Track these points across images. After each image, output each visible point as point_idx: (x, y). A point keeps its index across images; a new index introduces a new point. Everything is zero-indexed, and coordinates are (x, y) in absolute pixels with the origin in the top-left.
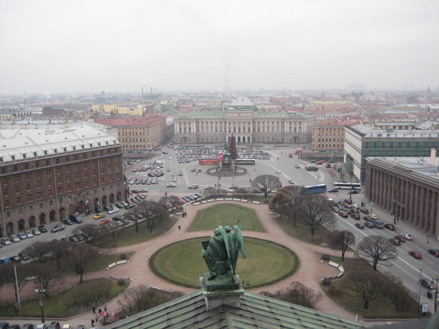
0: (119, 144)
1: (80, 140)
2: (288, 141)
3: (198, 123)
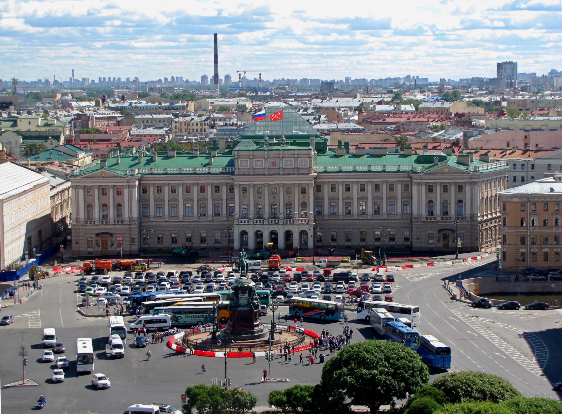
3: (145, 191)
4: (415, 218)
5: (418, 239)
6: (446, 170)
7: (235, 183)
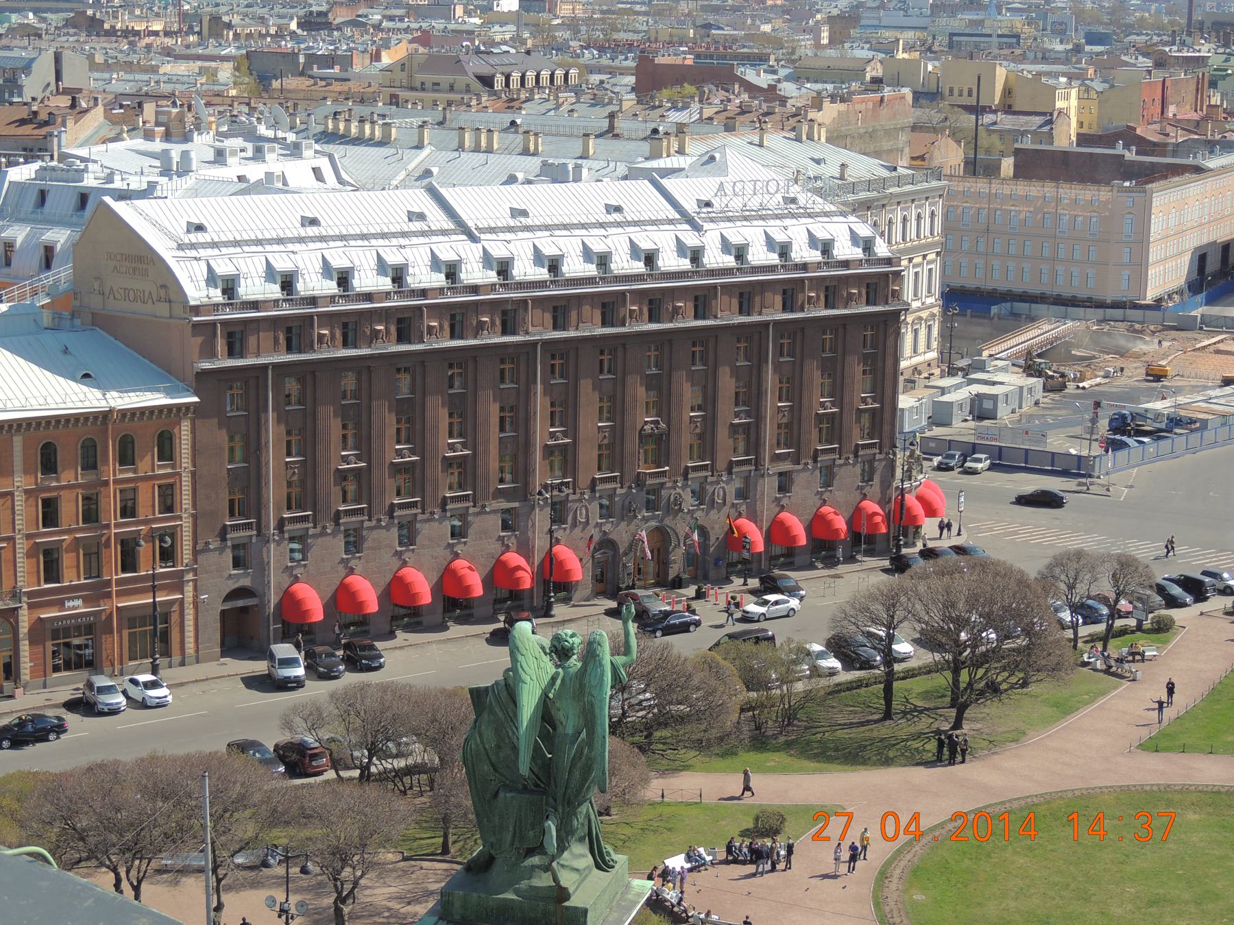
0: (888, 261)
1: (690, 221)
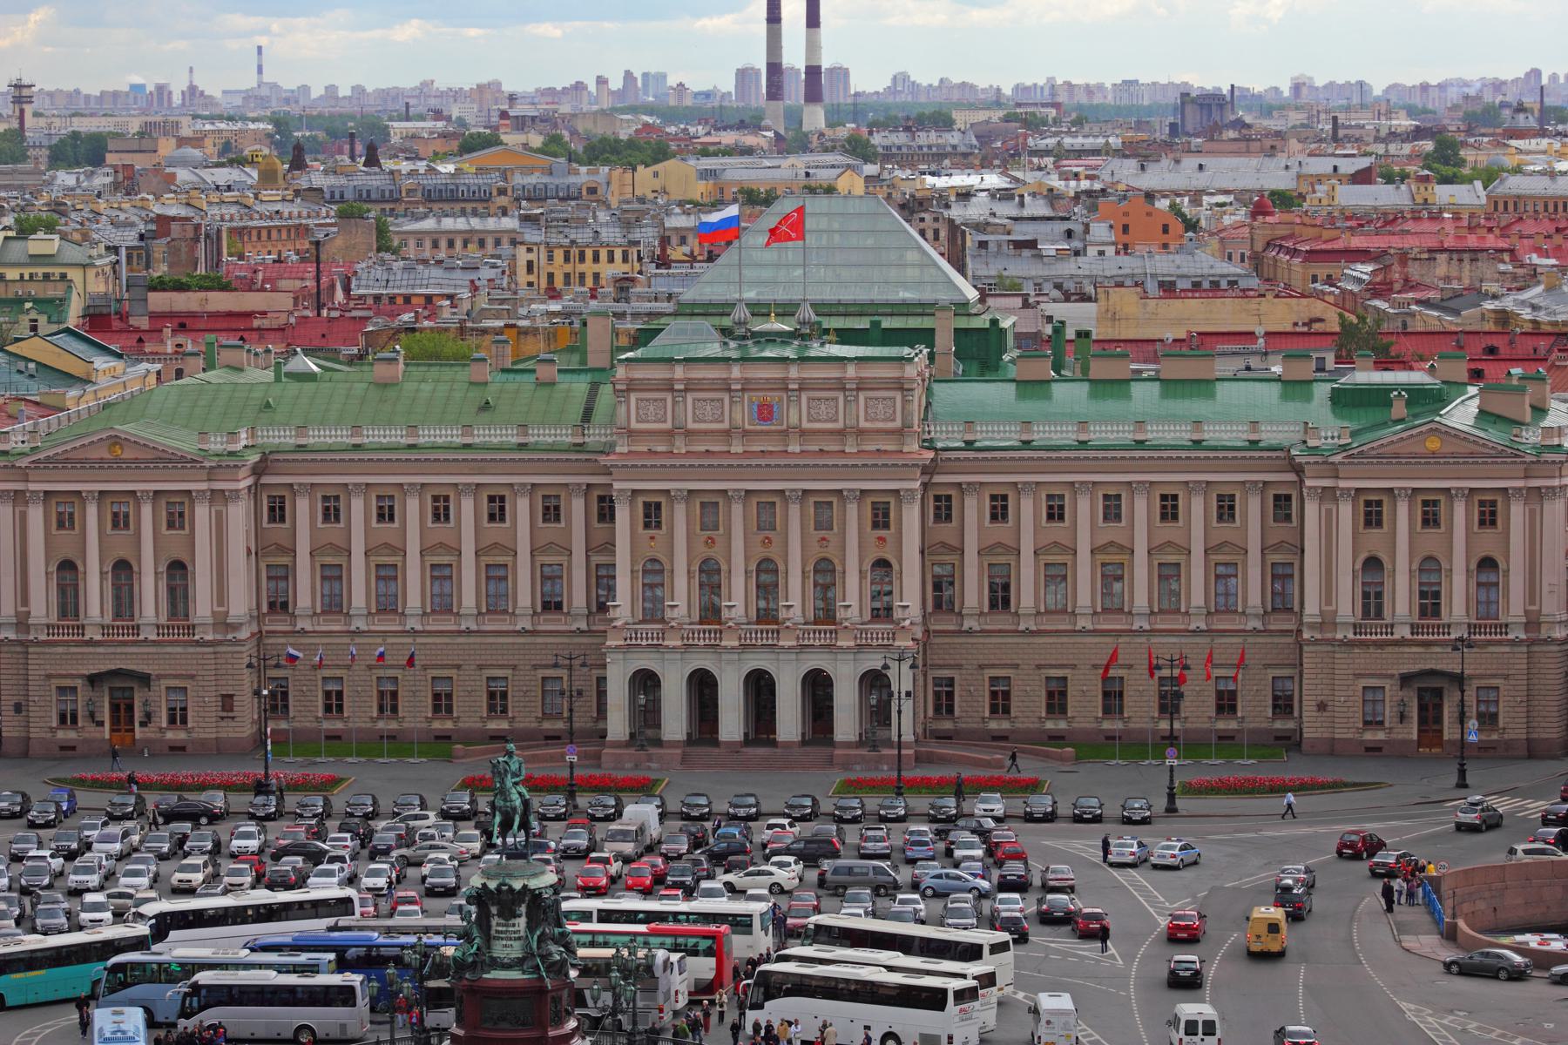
2: (1347, 727)
3: (278, 511)
4: (1312, 626)
5: (1322, 707)
6: (1433, 444)
7: (617, 485)
